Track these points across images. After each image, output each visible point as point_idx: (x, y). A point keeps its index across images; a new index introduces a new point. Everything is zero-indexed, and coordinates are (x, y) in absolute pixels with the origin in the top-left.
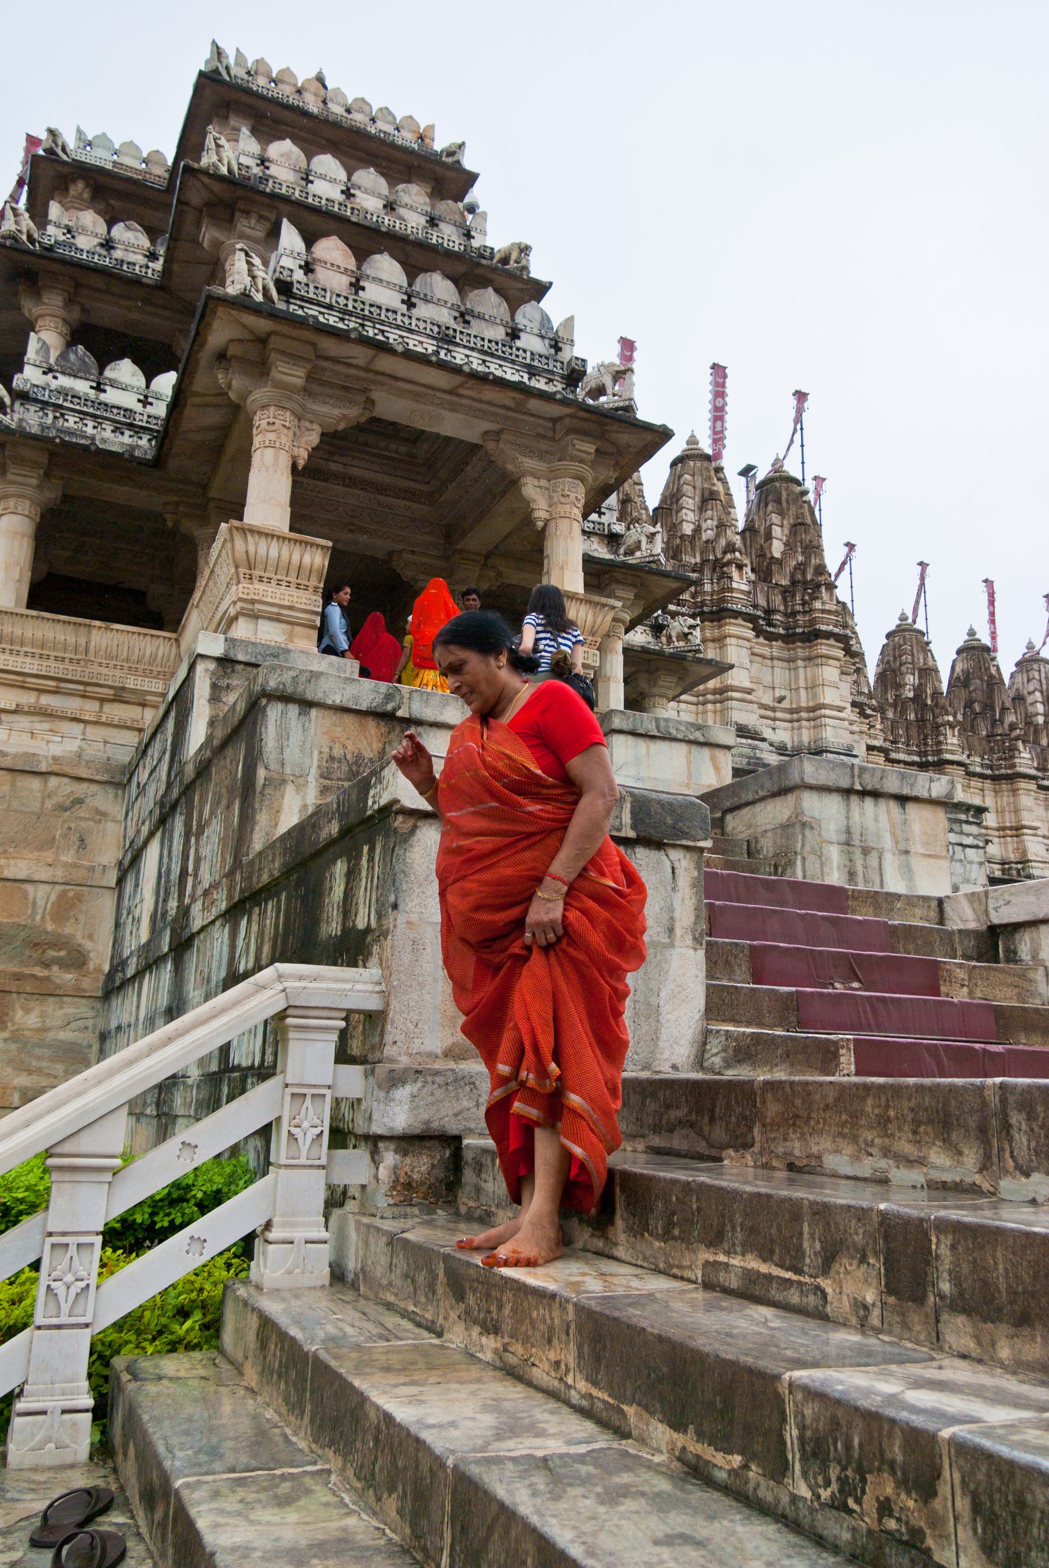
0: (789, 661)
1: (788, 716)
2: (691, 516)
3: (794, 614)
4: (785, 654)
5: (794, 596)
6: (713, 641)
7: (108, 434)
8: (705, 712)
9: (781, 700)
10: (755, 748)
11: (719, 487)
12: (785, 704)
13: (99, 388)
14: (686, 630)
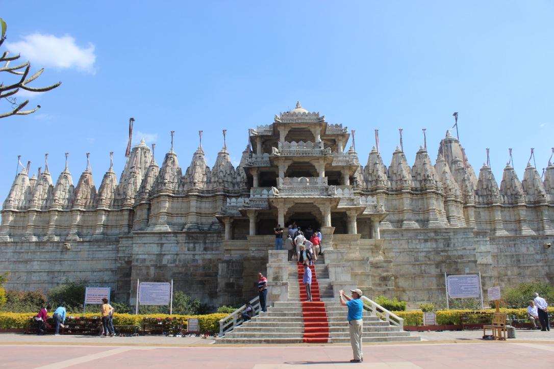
7: (263, 203)
9: (420, 209)
13: (261, 196)
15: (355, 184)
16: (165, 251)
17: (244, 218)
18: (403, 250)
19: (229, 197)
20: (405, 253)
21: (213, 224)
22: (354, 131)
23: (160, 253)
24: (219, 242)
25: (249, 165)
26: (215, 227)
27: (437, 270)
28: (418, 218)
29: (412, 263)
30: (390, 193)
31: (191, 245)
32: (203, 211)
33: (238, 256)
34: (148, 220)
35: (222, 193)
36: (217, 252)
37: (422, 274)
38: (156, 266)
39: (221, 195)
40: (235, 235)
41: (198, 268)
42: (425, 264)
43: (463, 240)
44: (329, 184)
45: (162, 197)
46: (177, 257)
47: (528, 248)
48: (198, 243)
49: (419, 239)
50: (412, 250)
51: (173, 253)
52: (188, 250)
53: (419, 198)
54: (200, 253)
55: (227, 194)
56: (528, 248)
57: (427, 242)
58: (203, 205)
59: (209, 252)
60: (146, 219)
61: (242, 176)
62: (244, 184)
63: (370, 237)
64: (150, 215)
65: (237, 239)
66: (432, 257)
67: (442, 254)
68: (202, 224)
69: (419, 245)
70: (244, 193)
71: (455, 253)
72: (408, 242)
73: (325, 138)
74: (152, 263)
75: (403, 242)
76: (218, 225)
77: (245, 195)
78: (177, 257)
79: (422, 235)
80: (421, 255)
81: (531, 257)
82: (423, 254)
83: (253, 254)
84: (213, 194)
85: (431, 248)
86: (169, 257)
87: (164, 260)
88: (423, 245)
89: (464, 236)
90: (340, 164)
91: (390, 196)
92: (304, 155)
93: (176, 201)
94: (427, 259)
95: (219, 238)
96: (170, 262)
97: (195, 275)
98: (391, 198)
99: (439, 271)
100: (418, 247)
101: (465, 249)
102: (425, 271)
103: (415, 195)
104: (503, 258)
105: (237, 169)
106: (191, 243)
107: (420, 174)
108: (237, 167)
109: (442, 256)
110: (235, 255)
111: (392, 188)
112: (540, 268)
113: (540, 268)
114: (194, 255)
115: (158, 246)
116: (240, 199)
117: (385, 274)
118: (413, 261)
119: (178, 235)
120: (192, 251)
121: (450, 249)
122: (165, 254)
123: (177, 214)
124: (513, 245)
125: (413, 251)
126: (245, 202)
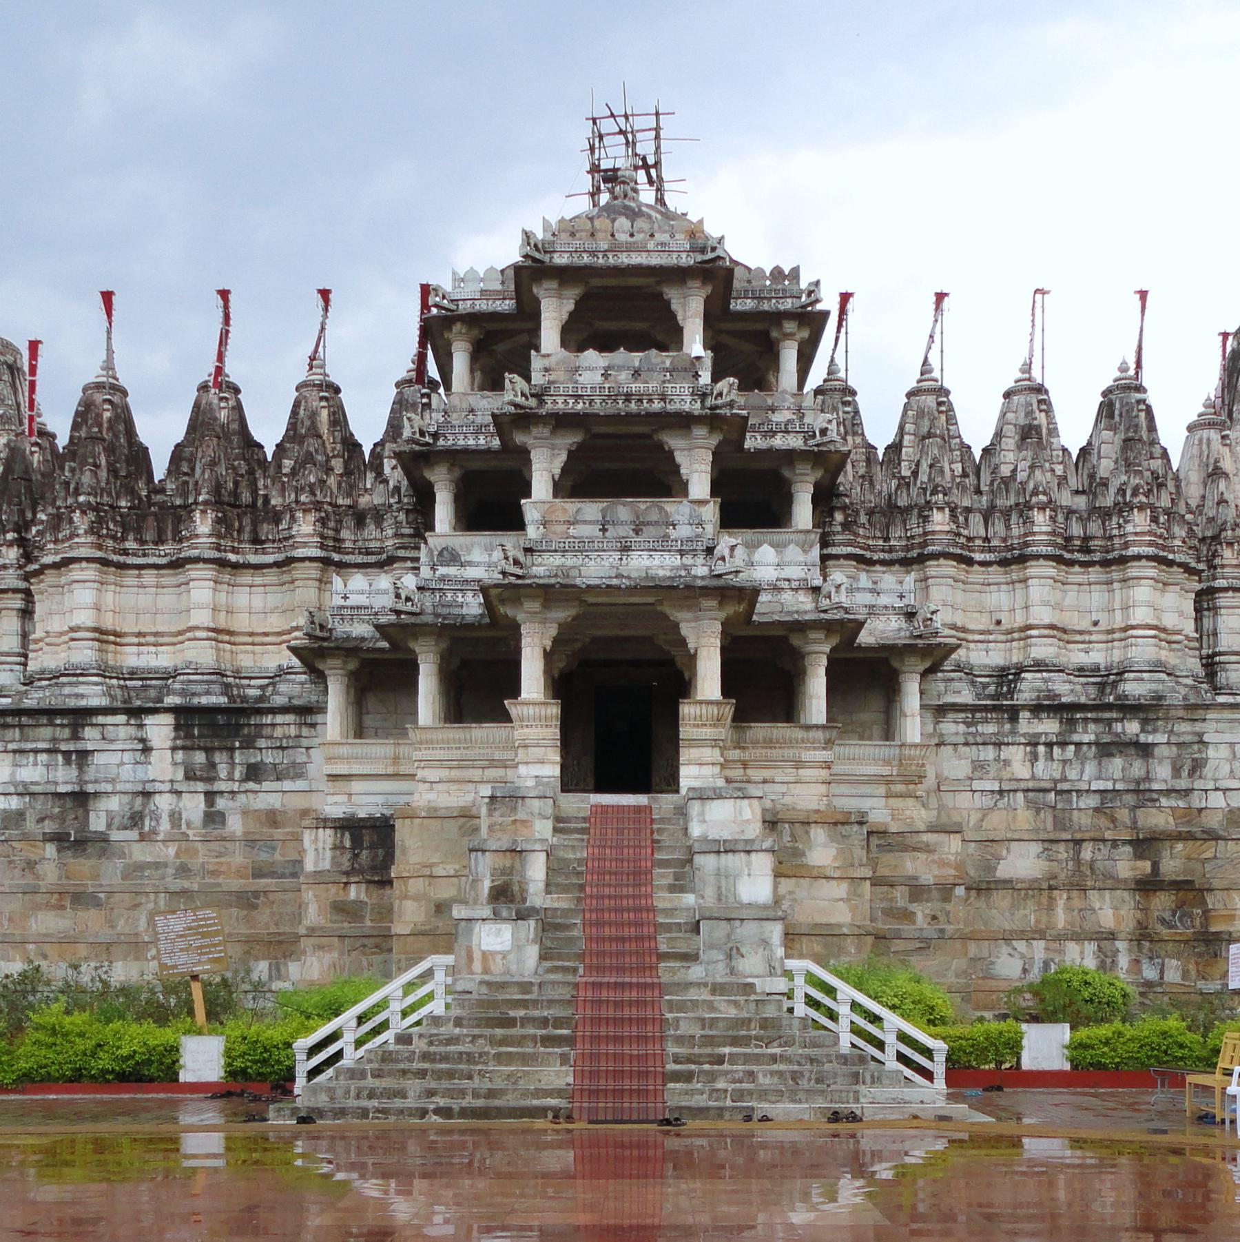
0: (1107, 583)
1: (1103, 637)
2: (1010, 456)
3: (1111, 538)
4: (1103, 577)
5: (1110, 519)
6: (1020, 582)
8: (1011, 650)
9: (1096, 624)
10: (1045, 681)
11: (1041, 419)
12: (1103, 626)
14: (929, 616)
15: (839, 517)
16: (96, 781)
17: (400, 656)
18: (1013, 786)
19: (341, 566)
20: (1020, 795)
21: (282, 673)
22: (851, 295)
23: (77, 789)
24: (305, 742)
25: (417, 443)
26: (285, 692)
27: (1140, 863)
28: (1078, 657)
29: (1043, 836)
30: (978, 557)
31: (200, 757)
32: (241, 623)
33: (380, 800)
34: (26, 656)
35: (318, 553)
36: (300, 784)
37: (1080, 882)
38: (59, 839)
39: (311, 559)
40: (368, 720)
41: (228, 845)
42: (1094, 840)
44: (729, 521)
45: (76, 566)
46: (144, 805)
48: (226, 748)
49: (1078, 745)
50: (1048, 785)
51: (129, 787)
52: (188, 777)
53: (1093, 577)
54: (236, 787)
55: (336, 557)
57: (1111, 755)
58: (242, 598)
59: (267, 785)
60: (19, 655)
61: (391, 484)
62: (402, 516)
63: (888, 733)
64: (32, 637)
65: (376, 735)
66: (1123, 815)
67: (1164, 802)
68: (237, 674)
69: (1077, 766)
70: (401, 553)
72: (1034, 758)
73: (729, 326)
74: (49, 827)
75: (1016, 754)
76: (303, 677)
77: (404, 559)
78: (144, 805)
79: (1092, 727)
80: (1082, 805)
82: (1093, 801)
83: (432, 796)
84: (280, 557)
85: (1123, 779)
86: (114, 804)
87: (92, 815)
88: (1090, 769)
90: (778, 442)
91: (976, 567)
92: (633, 406)
93: (134, 581)
94: (1103, 822)
95: (305, 731)
96: (117, 821)
97: (214, 873)
98: (980, 578)
99: (1149, 870)
100: (1072, 774)
103: (1077, 569)
105: (373, 451)
106: (200, 748)
107: (1105, 483)
108: (376, 445)
110: (366, 801)
111: (987, 539)
114: (210, 796)
115: (68, 761)
116: (384, 581)
118: (1050, 826)
119: (149, 720)
120: (201, 779)
121: (1198, 784)
122: (97, 794)
123: (139, 634)
125: (1049, 791)
126: (398, 596)
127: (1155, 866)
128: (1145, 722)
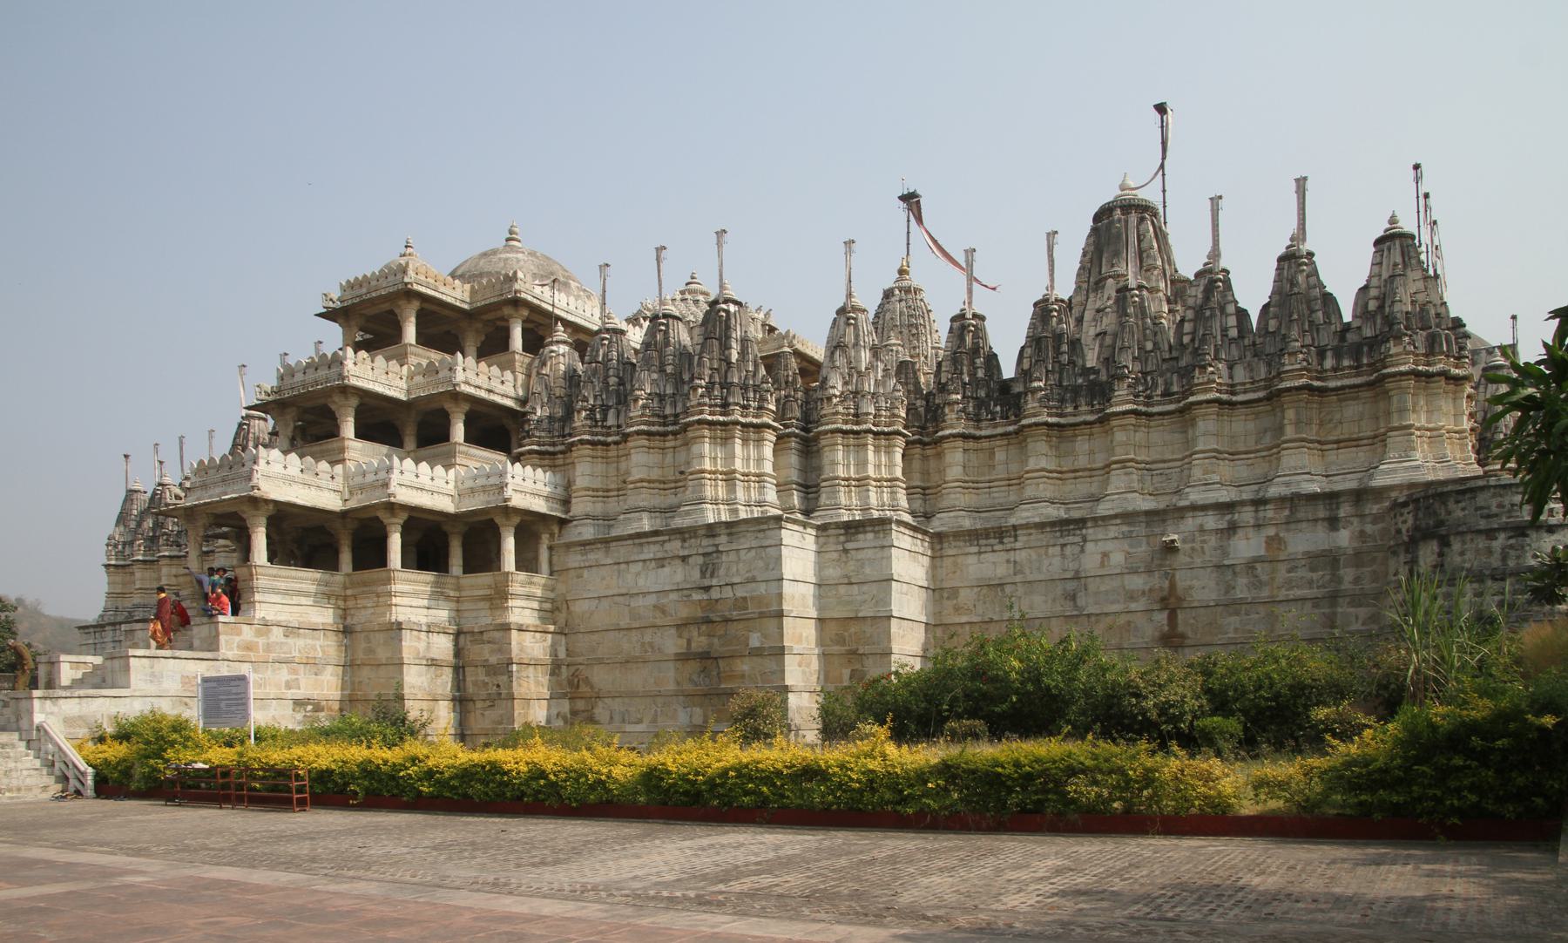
43: (753, 553)
47: (1105, 555)
56: (1105, 555)
67: (696, 596)
71: (728, 593)
81: (1116, 583)
82: (651, 600)
89: (754, 544)
94: (658, 614)
101: (753, 580)
102: (651, 644)
104: (1021, 590)
109: (693, 602)
112: (1140, 620)
113: (1140, 620)
117: (493, 660)
121: (714, 582)
124: (1058, 548)
127: (689, 642)
128: (684, 541)
